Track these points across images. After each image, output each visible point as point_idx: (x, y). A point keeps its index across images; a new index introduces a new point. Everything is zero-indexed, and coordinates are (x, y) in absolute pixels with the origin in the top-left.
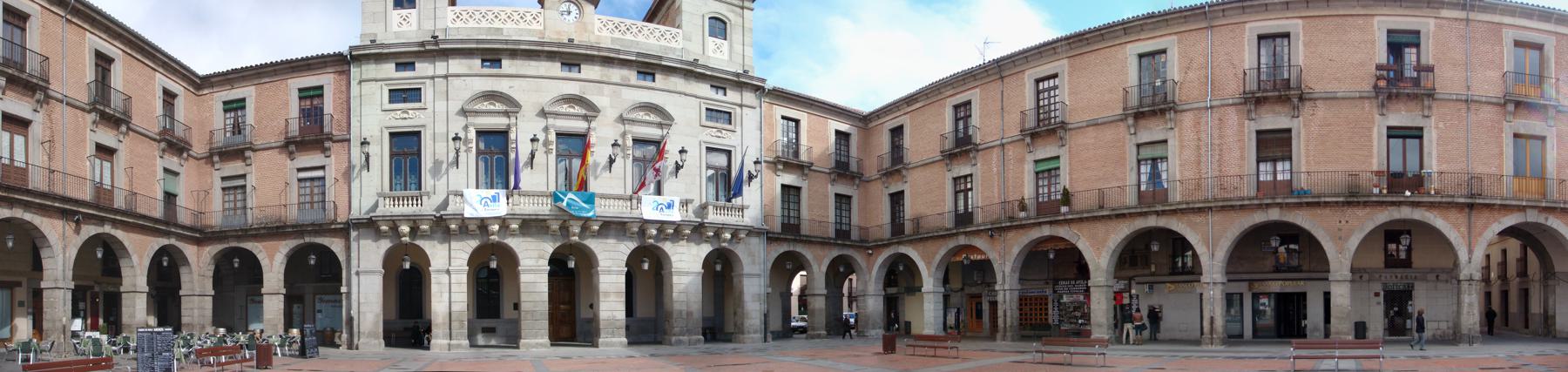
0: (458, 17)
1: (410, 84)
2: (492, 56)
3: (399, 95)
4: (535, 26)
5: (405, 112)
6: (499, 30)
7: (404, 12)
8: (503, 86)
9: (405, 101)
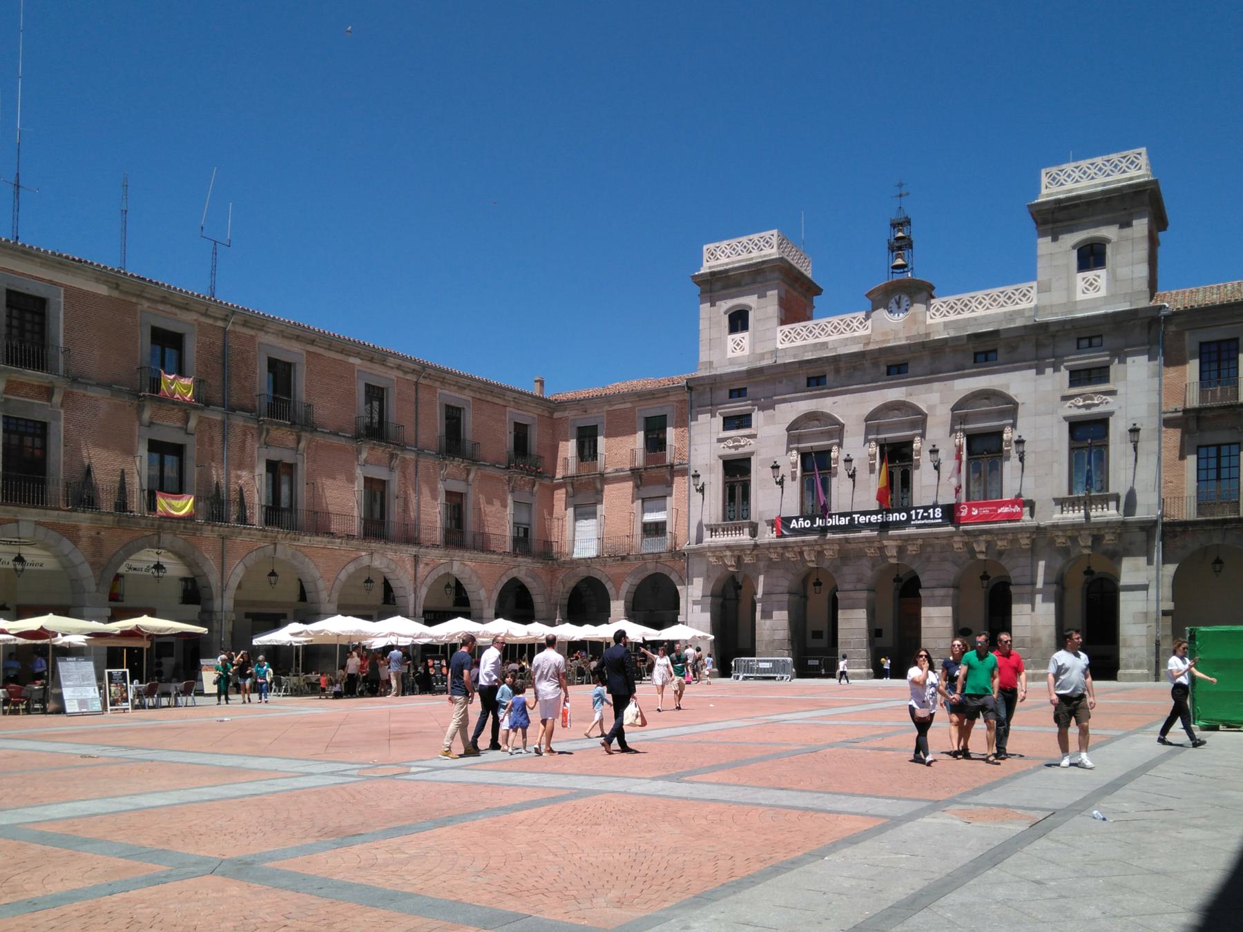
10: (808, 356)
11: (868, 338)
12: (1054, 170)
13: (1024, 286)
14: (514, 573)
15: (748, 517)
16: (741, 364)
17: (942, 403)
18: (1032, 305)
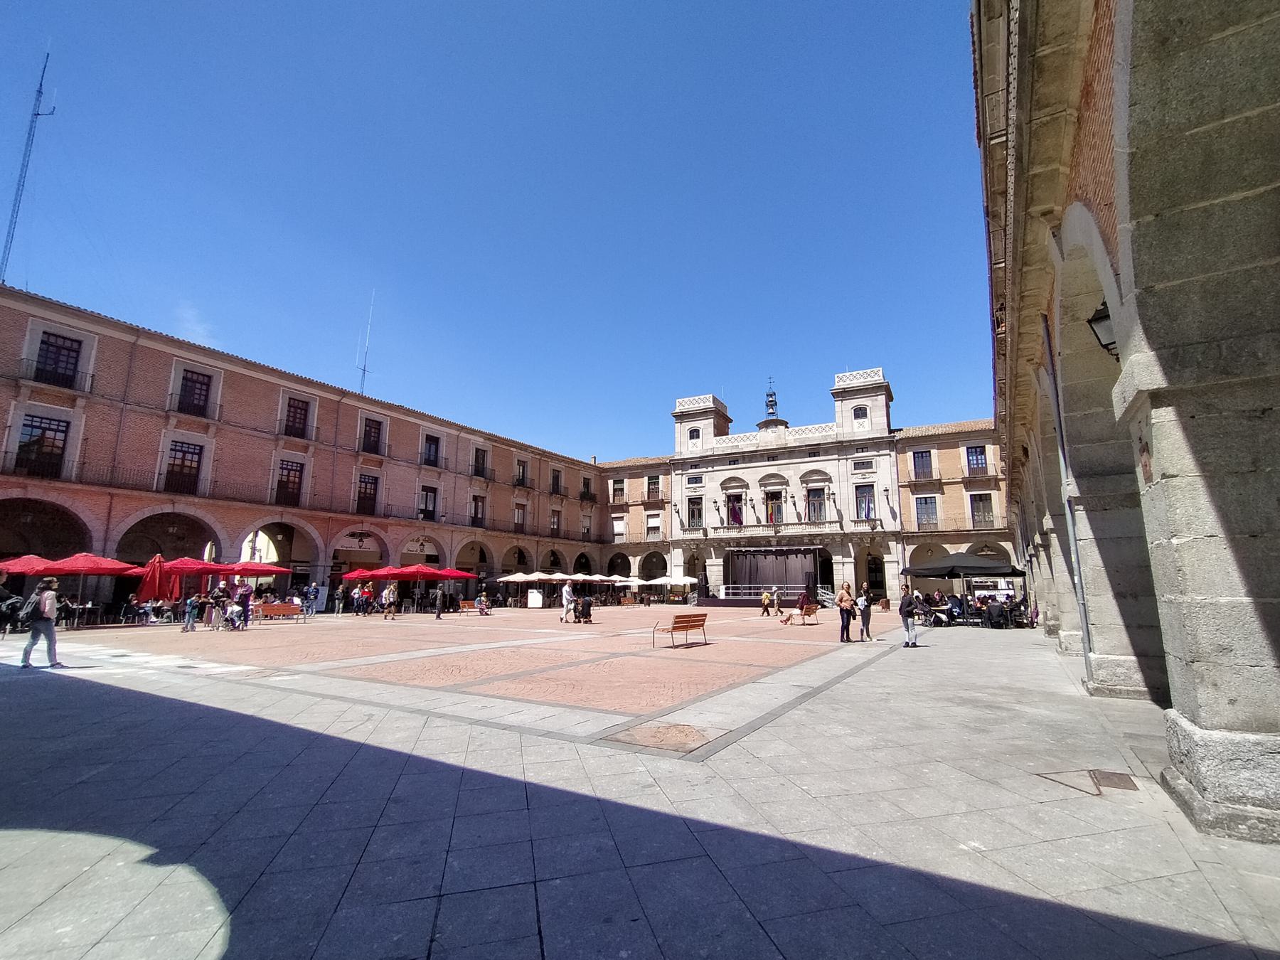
2: (734, 459)
3: (690, 481)
4: (754, 442)
11: (758, 444)
12: (841, 375)
13: (830, 424)
14: (583, 550)
15: (702, 525)
16: (697, 454)
17: (795, 475)
18: (835, 433)
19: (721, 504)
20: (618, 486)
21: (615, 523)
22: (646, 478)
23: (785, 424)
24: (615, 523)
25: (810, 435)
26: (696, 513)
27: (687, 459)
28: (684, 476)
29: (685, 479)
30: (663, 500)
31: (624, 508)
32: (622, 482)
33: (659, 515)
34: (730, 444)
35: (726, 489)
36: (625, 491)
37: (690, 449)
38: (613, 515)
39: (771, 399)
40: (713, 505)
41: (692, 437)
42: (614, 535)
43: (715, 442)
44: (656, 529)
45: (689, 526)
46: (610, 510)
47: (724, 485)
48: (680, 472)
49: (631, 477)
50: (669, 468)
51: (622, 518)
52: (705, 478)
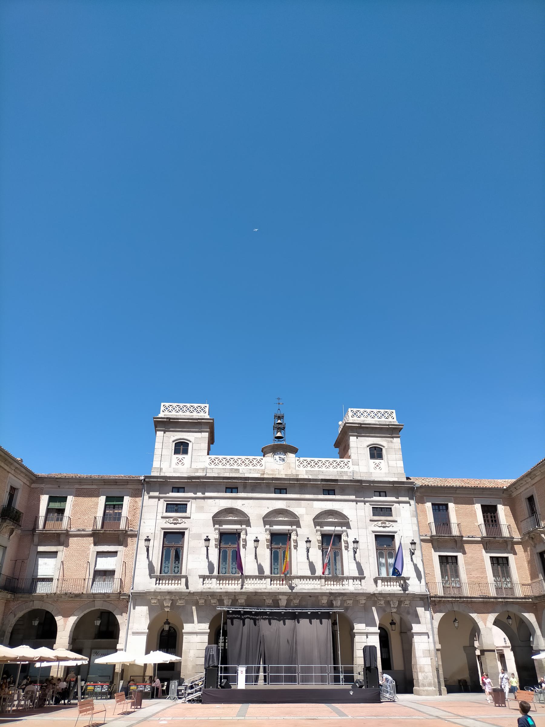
0: (213, 462)
1: (180, 501)
5: (176, 519)
6: (237, 470)
7: (180, 456)
8: (237, 504)
9: (176, 511)
10: (227, 475)
19: (213, 543)
20: (56, 505)
21: (42, 561)
22: (102, 500)
23: (294, 450)
24: (42, 561)
25: (324, 469)
26: (173, 553)
27: (170, 478)
28: (162, 500)
29: (162, 505)
30: (126, 531)
31: (62, 539)
32: (64, 499)
33: (116, 552)
34: (228, 466)
35: (220, 523)
36: (67, 513)
37: (174, 465)
38: (41, 549)
39: (279, 421)
40: (203, 543)
41: (177, 452)
42: (35, 580)
43: (208, 461)
44: (109, 574)
45: (160, 573)
46: (36, 539)
47: (217, 519)
48: (156, 494)
49: (79, 494)
50: (140, 487)
51: (54, 554)
52: (192, 506)
